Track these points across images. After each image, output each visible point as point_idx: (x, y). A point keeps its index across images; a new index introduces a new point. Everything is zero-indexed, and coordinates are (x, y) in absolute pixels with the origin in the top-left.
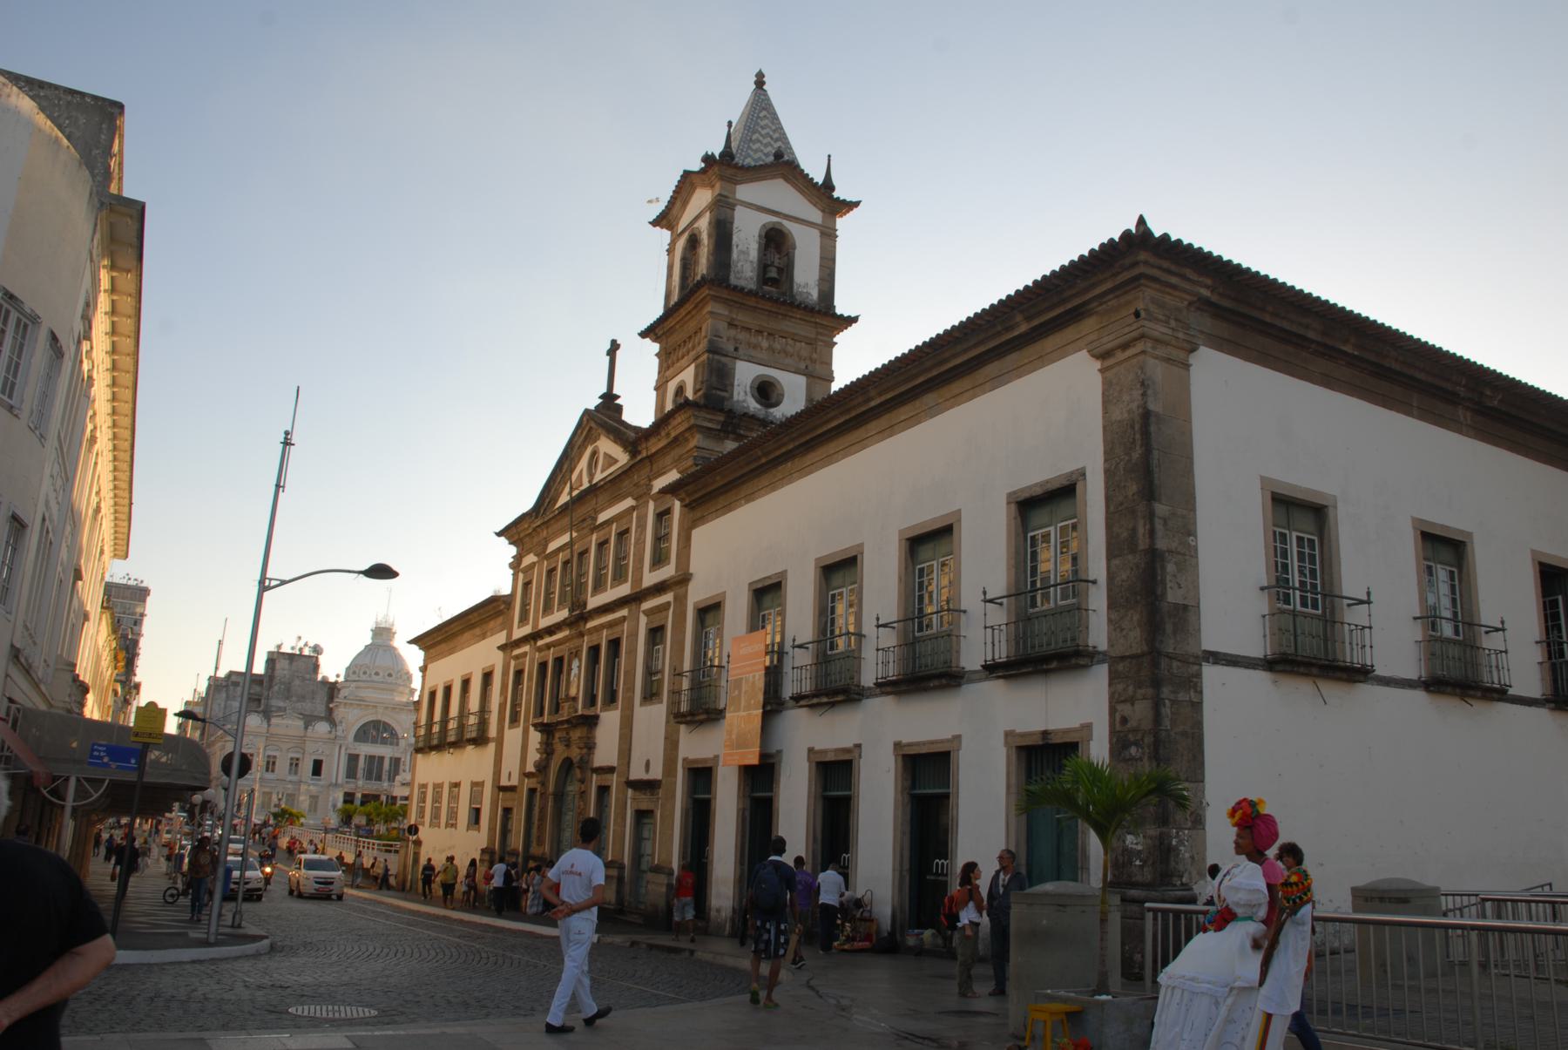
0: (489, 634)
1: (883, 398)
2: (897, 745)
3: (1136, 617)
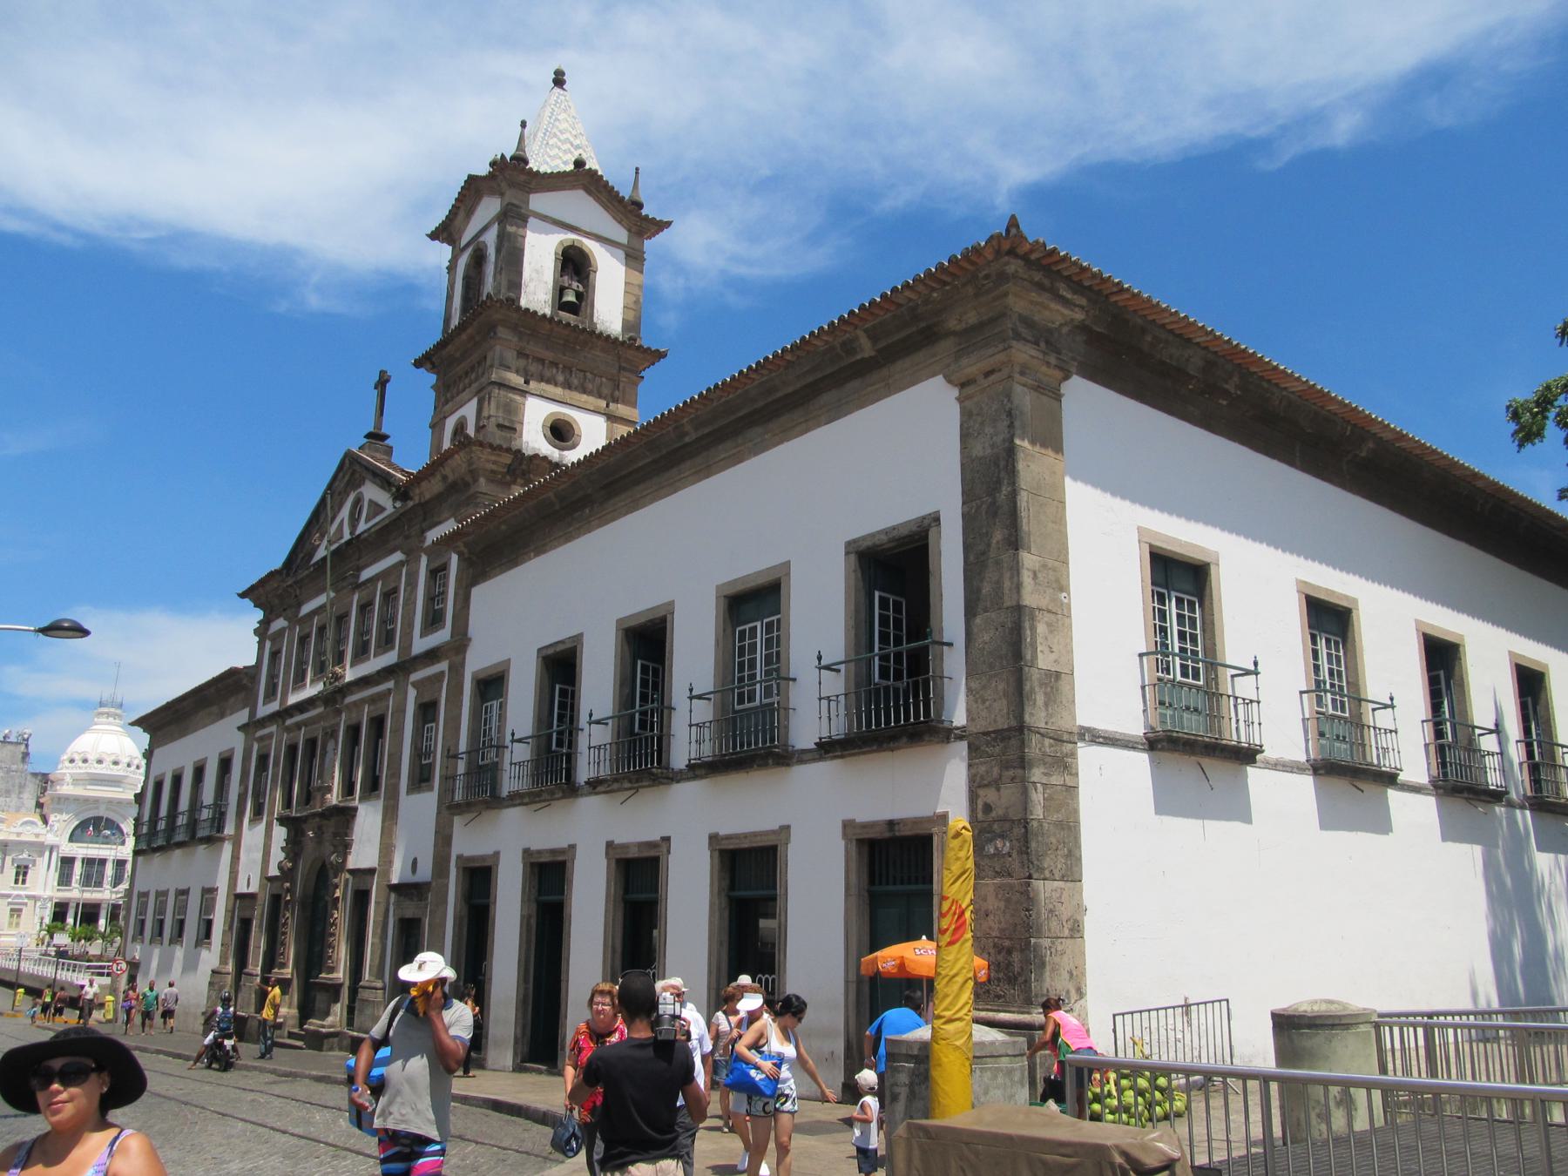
0: (228, 712)
1: (700, 433)
2: (714, 838)
3: (1001, 687)
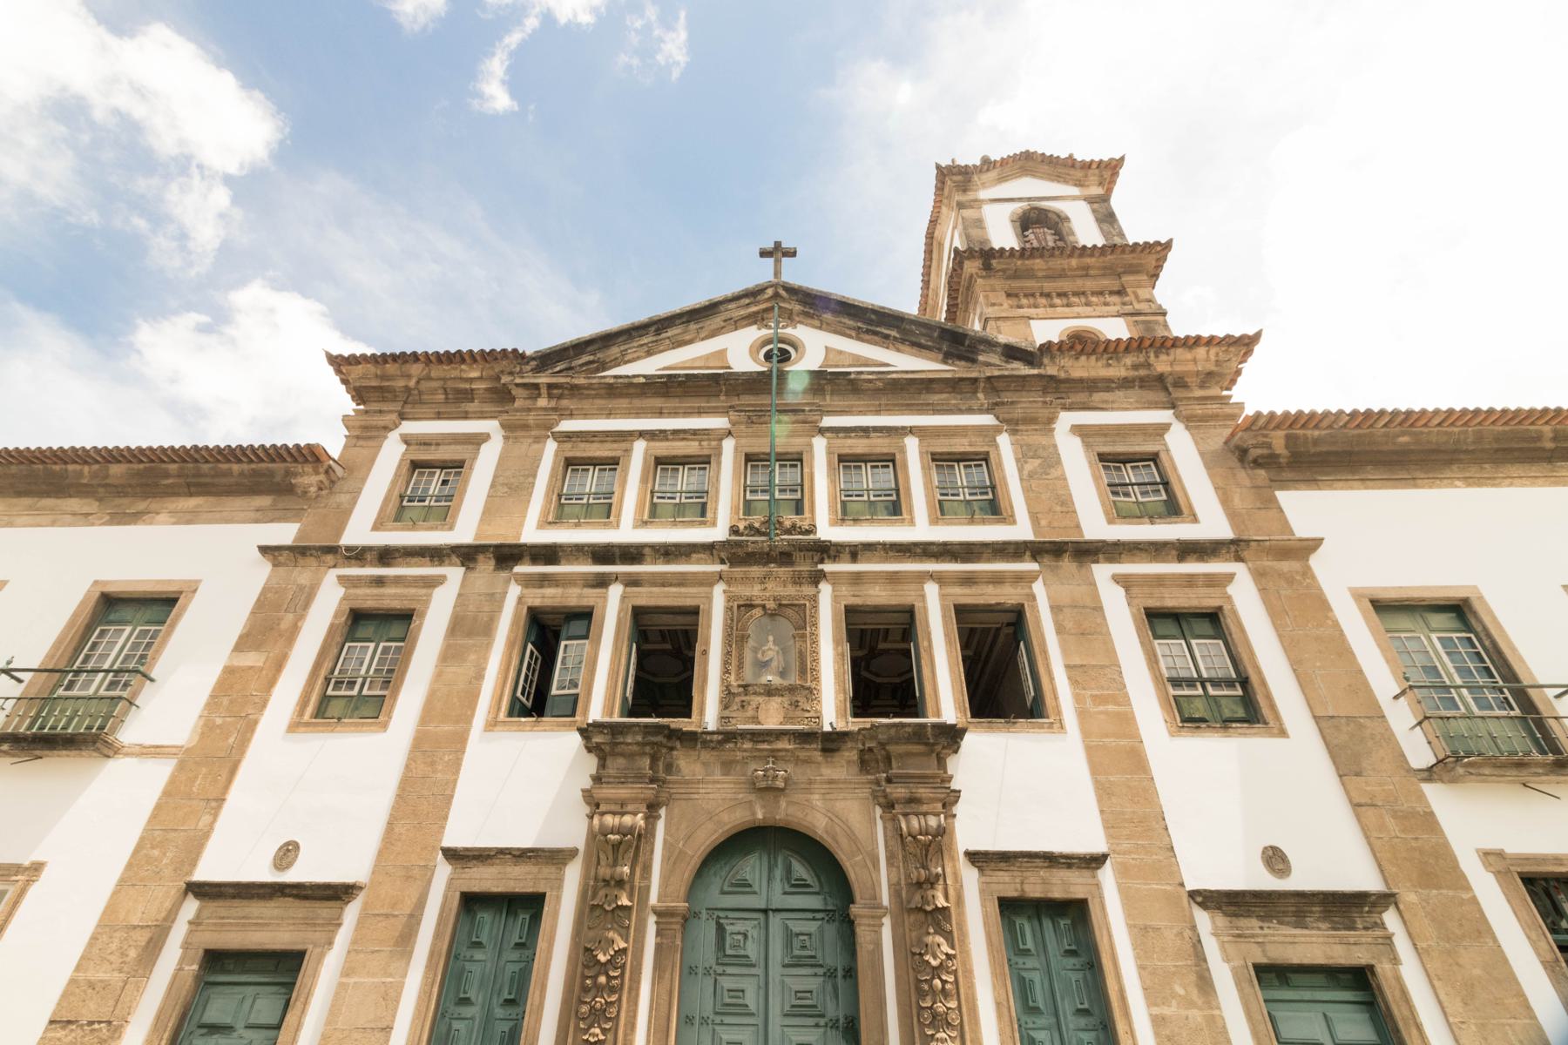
0: (162, 517)
